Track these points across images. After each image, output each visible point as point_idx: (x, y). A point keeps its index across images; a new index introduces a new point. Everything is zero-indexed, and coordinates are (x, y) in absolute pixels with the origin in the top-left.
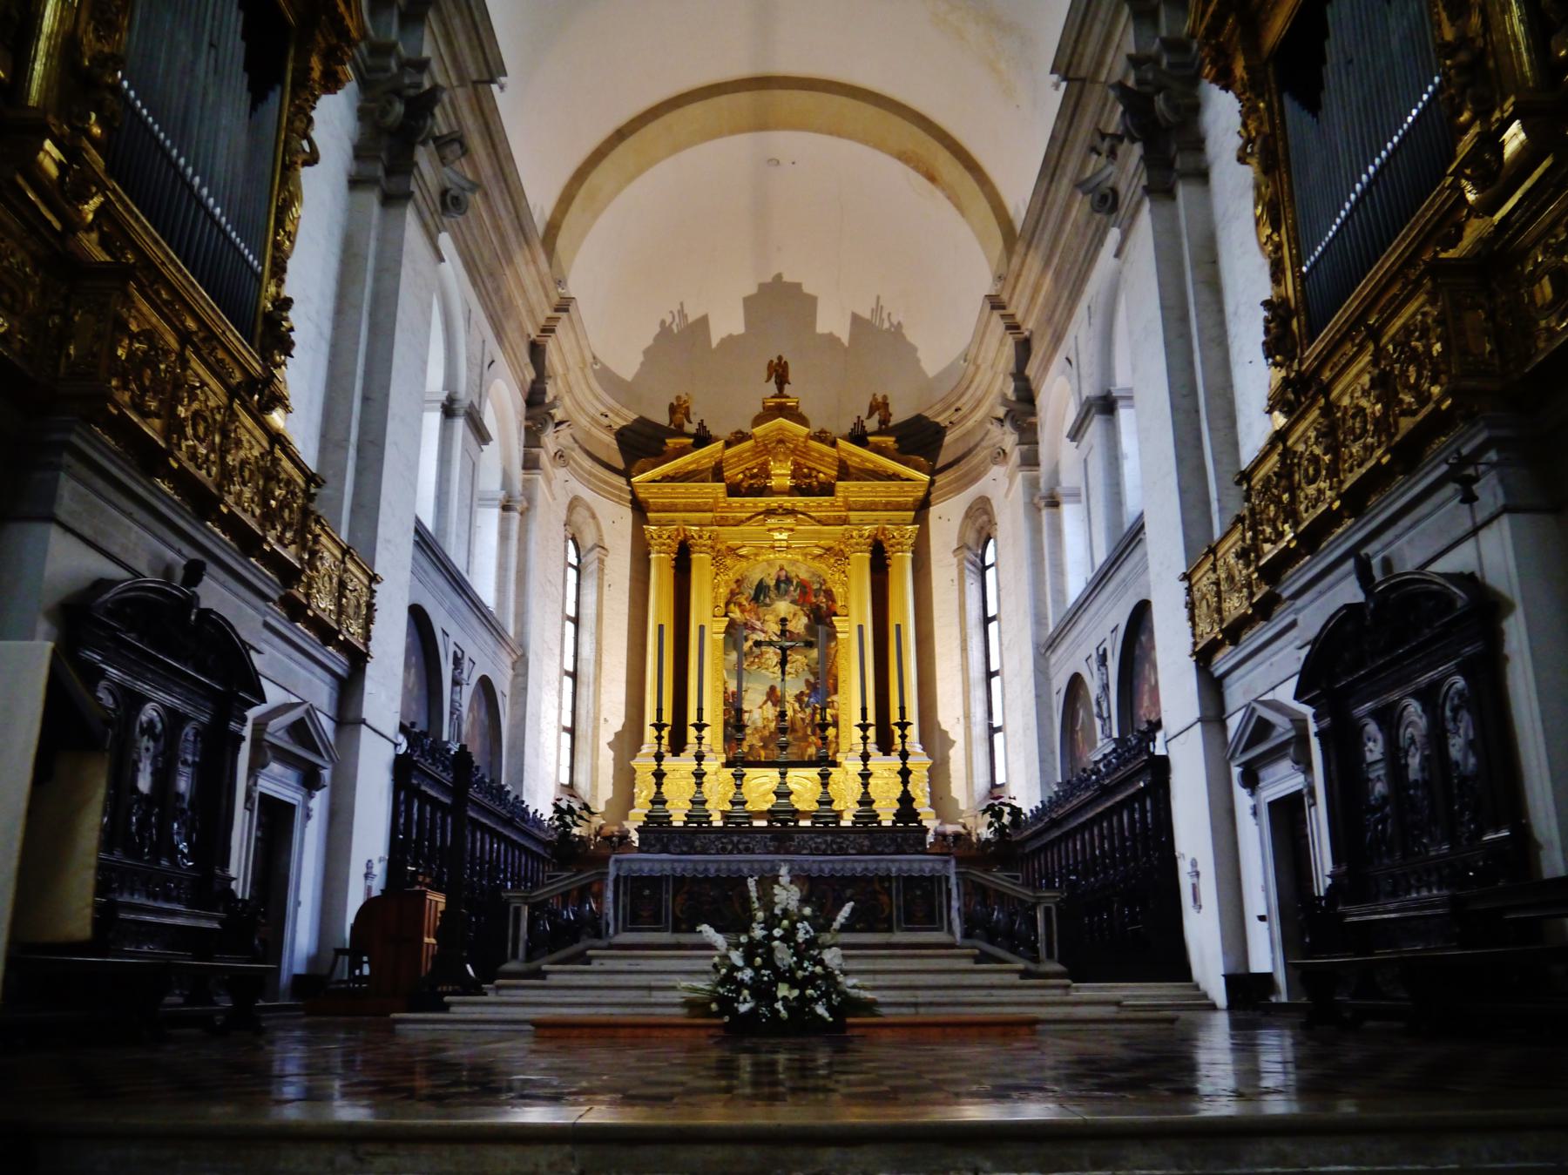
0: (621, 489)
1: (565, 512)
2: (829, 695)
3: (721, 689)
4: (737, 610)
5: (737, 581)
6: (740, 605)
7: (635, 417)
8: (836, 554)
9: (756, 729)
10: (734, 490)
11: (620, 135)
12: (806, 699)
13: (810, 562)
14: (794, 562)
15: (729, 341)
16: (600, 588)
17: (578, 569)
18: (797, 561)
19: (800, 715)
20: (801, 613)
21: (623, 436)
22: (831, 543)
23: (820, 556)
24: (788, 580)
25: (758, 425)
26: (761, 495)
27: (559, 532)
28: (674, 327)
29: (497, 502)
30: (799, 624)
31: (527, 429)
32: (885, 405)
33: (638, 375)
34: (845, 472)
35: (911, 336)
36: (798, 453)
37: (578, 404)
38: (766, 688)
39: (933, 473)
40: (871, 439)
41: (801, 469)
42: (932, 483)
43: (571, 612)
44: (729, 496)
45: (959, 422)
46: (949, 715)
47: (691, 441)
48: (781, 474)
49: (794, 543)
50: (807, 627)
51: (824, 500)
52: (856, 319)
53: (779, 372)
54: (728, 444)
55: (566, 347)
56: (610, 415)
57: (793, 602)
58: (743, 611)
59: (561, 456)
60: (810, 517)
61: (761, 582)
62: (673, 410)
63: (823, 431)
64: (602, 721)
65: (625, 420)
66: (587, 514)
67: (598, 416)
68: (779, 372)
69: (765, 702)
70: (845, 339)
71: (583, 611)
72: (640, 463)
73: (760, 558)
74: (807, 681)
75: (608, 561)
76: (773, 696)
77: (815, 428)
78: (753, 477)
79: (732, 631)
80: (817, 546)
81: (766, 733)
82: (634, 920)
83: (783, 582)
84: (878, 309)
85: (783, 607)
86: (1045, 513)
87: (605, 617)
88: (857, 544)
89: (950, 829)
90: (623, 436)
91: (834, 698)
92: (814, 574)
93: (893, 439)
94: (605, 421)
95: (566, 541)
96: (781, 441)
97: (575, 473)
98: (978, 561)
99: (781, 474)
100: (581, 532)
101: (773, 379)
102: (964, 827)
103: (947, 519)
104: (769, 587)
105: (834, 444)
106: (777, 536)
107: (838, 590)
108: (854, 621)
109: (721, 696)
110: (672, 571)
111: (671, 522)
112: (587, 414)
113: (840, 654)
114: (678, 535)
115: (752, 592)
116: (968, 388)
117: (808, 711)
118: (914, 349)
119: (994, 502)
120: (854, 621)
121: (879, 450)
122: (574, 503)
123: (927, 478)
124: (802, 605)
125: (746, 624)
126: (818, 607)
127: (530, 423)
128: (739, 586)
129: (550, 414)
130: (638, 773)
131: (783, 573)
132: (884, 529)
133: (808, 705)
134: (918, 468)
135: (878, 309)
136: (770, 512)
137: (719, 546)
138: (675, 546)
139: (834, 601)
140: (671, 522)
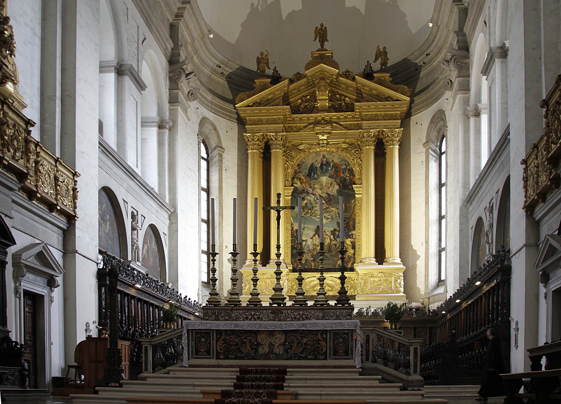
0: (231, 112)
1: (197, 127)
2: (350, 231)
3: (290, 228)
4: (299, 183)
5: (299, 165)
6: (300, 179)
7: (237, 66)
9: (309, 250)
10: (296, 110)
12: (337, 233)
13: (340, 152)
14: (331, 153)
16: (220, 171)
17: (207, 160)
18: (333, 152)
19: (334, 242)
20: (335, 183)
21: (230, 79)
22: (353, 141)
23: (346, 149)
24: (328, 164)
25: (309, 69)
26: (311, 112)
27: (195, 139)
28: (259, 7)
29: (155, 124)
31: (170, 78)
36: (333, 85)
37: (203, 61)
38: (314, 227)
40: (375, 75)
41: (335, 95)
42: (412, 102)
43: (205, 186)
44: (293, 114)
45: (429, 63)
47: (270, 80)
49: (331, 141)
50: (339, 192)
54: (291, 81)
55: (191, 26)
56: (222, 66)
57: (330, 177)
58: (301, 183)
59: (192, 94)
60: (340, 125)
61: (312, 164)
62: (259, 61)
63: (347, 71)
64: (224, 247)
65: (232, 69)
66: (211, 127)
67: (215, 66)
69: (314, 235)
71: (211, 185)
72: (240, 95)
73: (311, 151)
75: (225, 155)
76: (318, 231)
77: (343, 70)
78: (307, 101)
79: (296, 194)
80: (344, 142)
81: (315, 253)
83: (325, 165)
85: (324, 179)
87: (224, 188)
88: (367, 141)
90: (230, 79)
91: (353, 232)
92: (342, 160)
93: (389, 75)
94: (220, 70)
95: (199, 144)
96: (323, 79)
97: (202, 103)
100: (208, 139)
101: (318, 39)
104: (317, 168)
105: (354, 79)
106: (321, 137)
107: (356, 169)
109: (290, 232)
110: (261, 160)
112: (208, 66)
113: (357, 207)
114: (264, 138)
115: (307, 171)
116: (433, 41)
119: (446, 113)
122: (203, 121)
124: (335, 178)
125: (303, 190)
126: (345, 179)
127: (172, 75)
128: (299, 168)
129: (183, 69)
130: (244, 276)
131: (325, 159)
132: (383, 131)
133: (338, 237)
137: (287, 144)
138: (262, 145)
139: (354, 176)
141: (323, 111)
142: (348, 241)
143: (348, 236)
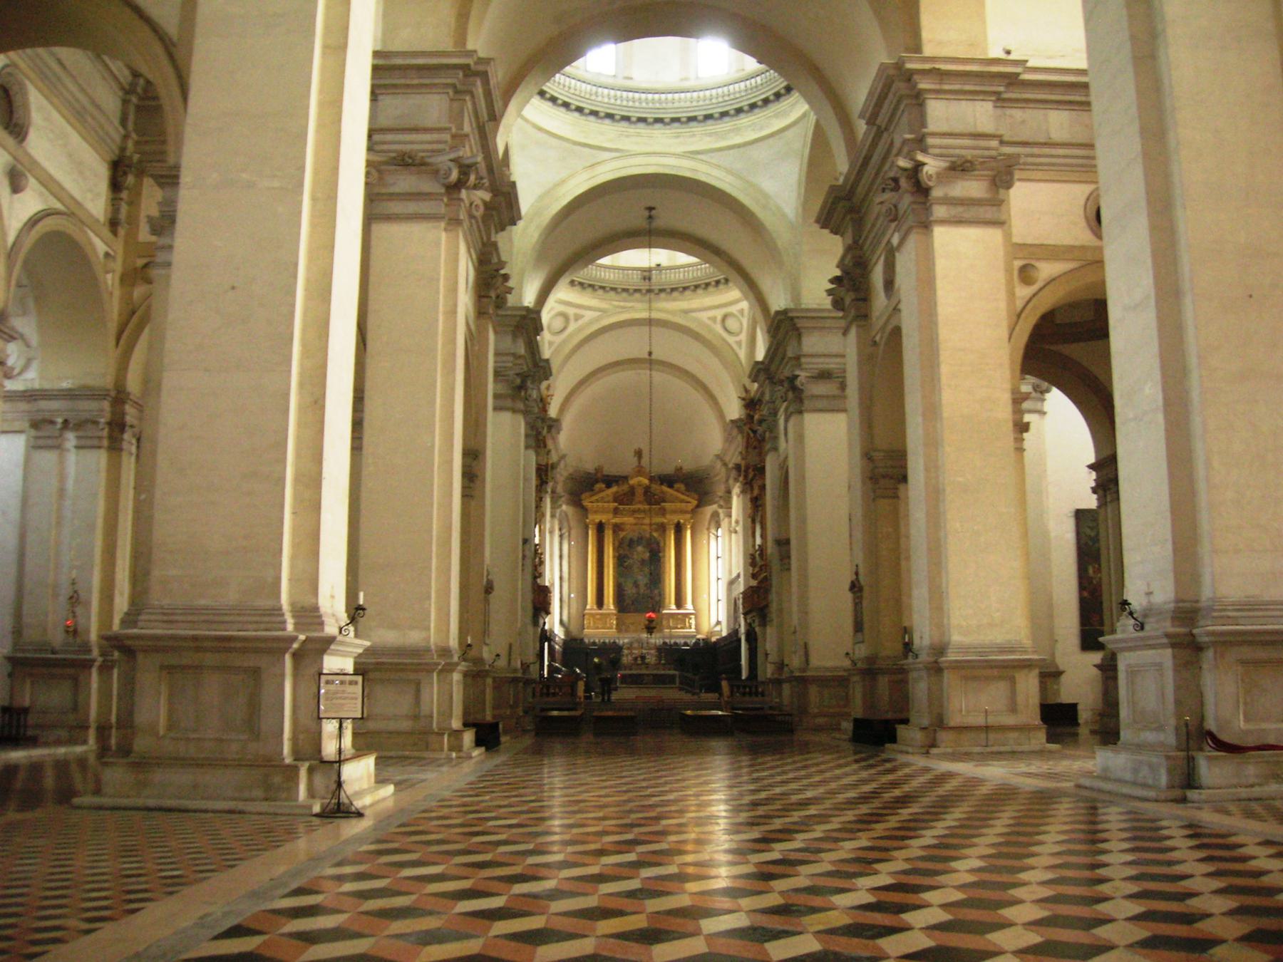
26: (631, 504)
32: (681, 468)
50: (650, 557)
53: (639, 454)
68: (639, 454)
76: (636, 585)
82: (622, 683)
83: (640, 539)
85: (640, 549)
86: (733, 535)
121: (678, 490)
136: (634, 512)
141: (640, 502)
142: (656, 592)
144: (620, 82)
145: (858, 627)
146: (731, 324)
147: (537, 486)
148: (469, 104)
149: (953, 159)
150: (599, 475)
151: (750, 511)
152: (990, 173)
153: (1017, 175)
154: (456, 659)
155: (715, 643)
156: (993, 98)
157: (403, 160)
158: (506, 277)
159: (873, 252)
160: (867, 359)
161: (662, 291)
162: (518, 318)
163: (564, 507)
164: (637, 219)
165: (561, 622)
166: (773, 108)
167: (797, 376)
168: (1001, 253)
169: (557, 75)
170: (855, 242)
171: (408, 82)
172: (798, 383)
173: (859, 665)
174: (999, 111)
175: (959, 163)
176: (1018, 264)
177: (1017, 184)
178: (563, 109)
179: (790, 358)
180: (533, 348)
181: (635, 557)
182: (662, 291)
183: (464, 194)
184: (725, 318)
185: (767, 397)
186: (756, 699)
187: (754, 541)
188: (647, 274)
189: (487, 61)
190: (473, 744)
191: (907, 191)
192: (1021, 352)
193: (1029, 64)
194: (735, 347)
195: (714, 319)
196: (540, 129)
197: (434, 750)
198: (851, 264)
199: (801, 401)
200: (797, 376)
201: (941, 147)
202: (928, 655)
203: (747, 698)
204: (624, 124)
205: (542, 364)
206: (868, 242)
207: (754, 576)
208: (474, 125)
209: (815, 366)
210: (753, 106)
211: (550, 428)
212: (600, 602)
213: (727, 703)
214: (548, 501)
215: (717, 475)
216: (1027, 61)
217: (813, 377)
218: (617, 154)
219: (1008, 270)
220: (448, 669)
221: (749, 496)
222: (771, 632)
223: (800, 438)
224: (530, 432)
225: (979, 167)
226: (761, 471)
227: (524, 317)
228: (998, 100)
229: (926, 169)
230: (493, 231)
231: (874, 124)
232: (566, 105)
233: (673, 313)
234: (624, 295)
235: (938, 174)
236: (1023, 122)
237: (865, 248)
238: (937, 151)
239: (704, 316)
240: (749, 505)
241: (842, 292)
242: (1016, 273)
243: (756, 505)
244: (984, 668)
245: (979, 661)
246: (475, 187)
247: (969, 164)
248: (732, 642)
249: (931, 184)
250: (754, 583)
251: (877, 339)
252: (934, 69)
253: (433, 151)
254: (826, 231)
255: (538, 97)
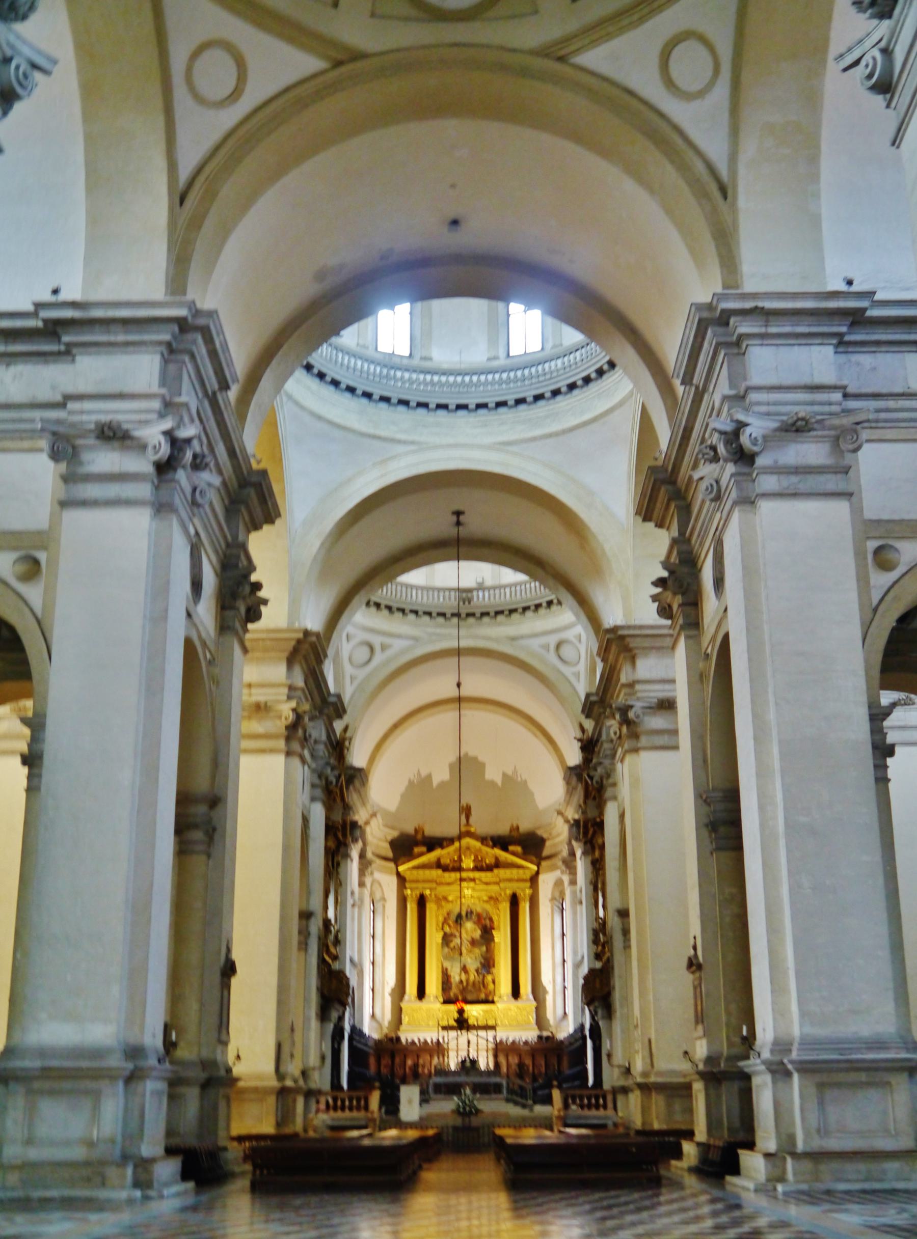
8: (494, 900)
11: (396, 726)
15: (442, 785)
21: (394, 844)
24: (472, 912)
28: (415, 781)
30: (477, 934)
32: (518, 828)
33: (398, 809)
34: (498, 864)
35: (532, 786)
39: (538, 865)
46: (546, 978)
48: (468, 863)
50: (482, 936)
51: (489, 874)
52: (505, 775)
57: (475, 923)
58: (450, 926)
68: (467, 811)
70: (499, 783)
74: (481, 963)
76: (464, 969)
83: (469, 914)
84: (515, 771)
86: (578, 907)
89: (545, 1034)
90: (394, 844)
98: (561, 907)
99: (468, 863)
102: (552, 1033)
103: (547, 881)
107: (495, 918)
108: (502, 938)
111: (417, 888)
117: (481, 977)
118: (532, 794)
120: (502, 938)
121: (514, 854)
123: (535, 868)
133: (481, 973)
134: (532, 862)
135: (515, 771)
140: (417, 888)
141: (468, 870)
142: (489, 978)
143: (489, 972)
144: (416, 362)
145: (699, 1018)
146: (566, 651)
147: (327, 849)
148: (190, 366)
149: (785, 418)
150: (419, 837)
151: (590, 876)
152: (833, 433)
153: (865, 435)
154: (152, 1062)
155: (562, 1042)
156: (834, 341)
157: (103, 432)
158: (258, 586)
159: (702, 544)
160: (697, 678)
161: (485, 614)
162: (293, 643)
163: (377, 875)
164: (442, 526)
165: (373, 1016)
166: (594, 387)
167: (631, 707)
168: (849, 533)
169: (325, 346)
170: (682, 532)
171: (112, 338)
172: (631, 715)
173: (701, 1067)
174: (842, 358)
175: (790, 421)
176: (872, 545)
177: (866, 447)
178: (348, 395)
179: (623, 685)
180: (315, 678)
181: (464, 935)
182: (485, 614)
183: (181, 475)
184: (558, 646)
185: (604, 737)
186: (594, 1112)
187: (597, 913)
188: (465, 594)
189: (212, 314)
190: (179, 1178)
191: (726, 461)
192: (878, 658)
193: (878, 297)
194: (573, 679)
195: (546, 647)
196: (319, 418)
197: (113, 1188)
198: (677, 561)
199: (635, 736)
200: (631, 707)
201: (768, 404)
202: (772, 1052)
203: (586, 1112)
204: (422, 411)
205: (332, 699)
206: (696, 534)
207: (598, 956)
208: (200, 395)
209: (652, 694)
210: (572, 387)
211: (350, 780)
212: (421, 993)
213: (559, 1118)
214: (353, 867)
215: (559, 835)
216: (875, 293)
217: (650, 708)
218: (412, 447)
219: (859, 554)
220: (132, 1078)
221: (589, 858)
222: (617, 1025)
223: (635, 782)
224: (317, 781)
225: (816, 426)
226: (599, 826)
227: (299, 642)
228: (841, 343)
229: (748, 430)
230: (241, 528)
231: (691, 384)
232: (351, 390)
233: (497, 640)
234: (441, 620)
235: (765, 437)
236: (874, 369)
237: (693, 541)
238: (764, 409)
239: (535, 643)
240: (590, 868)
241: (668, 596)
242: (870, 557)
243: (597, 866)
244: (848, 1070)
245: (838, 1061)
246: (198, 464)
247: (804, 423)
248: (576, 1040)
249: (756, 449)
250: (598, 965)
251: (709, 651)
252: (756, 308)
253: (140, 422)
254: (651, 525)
255: (304, 372)
